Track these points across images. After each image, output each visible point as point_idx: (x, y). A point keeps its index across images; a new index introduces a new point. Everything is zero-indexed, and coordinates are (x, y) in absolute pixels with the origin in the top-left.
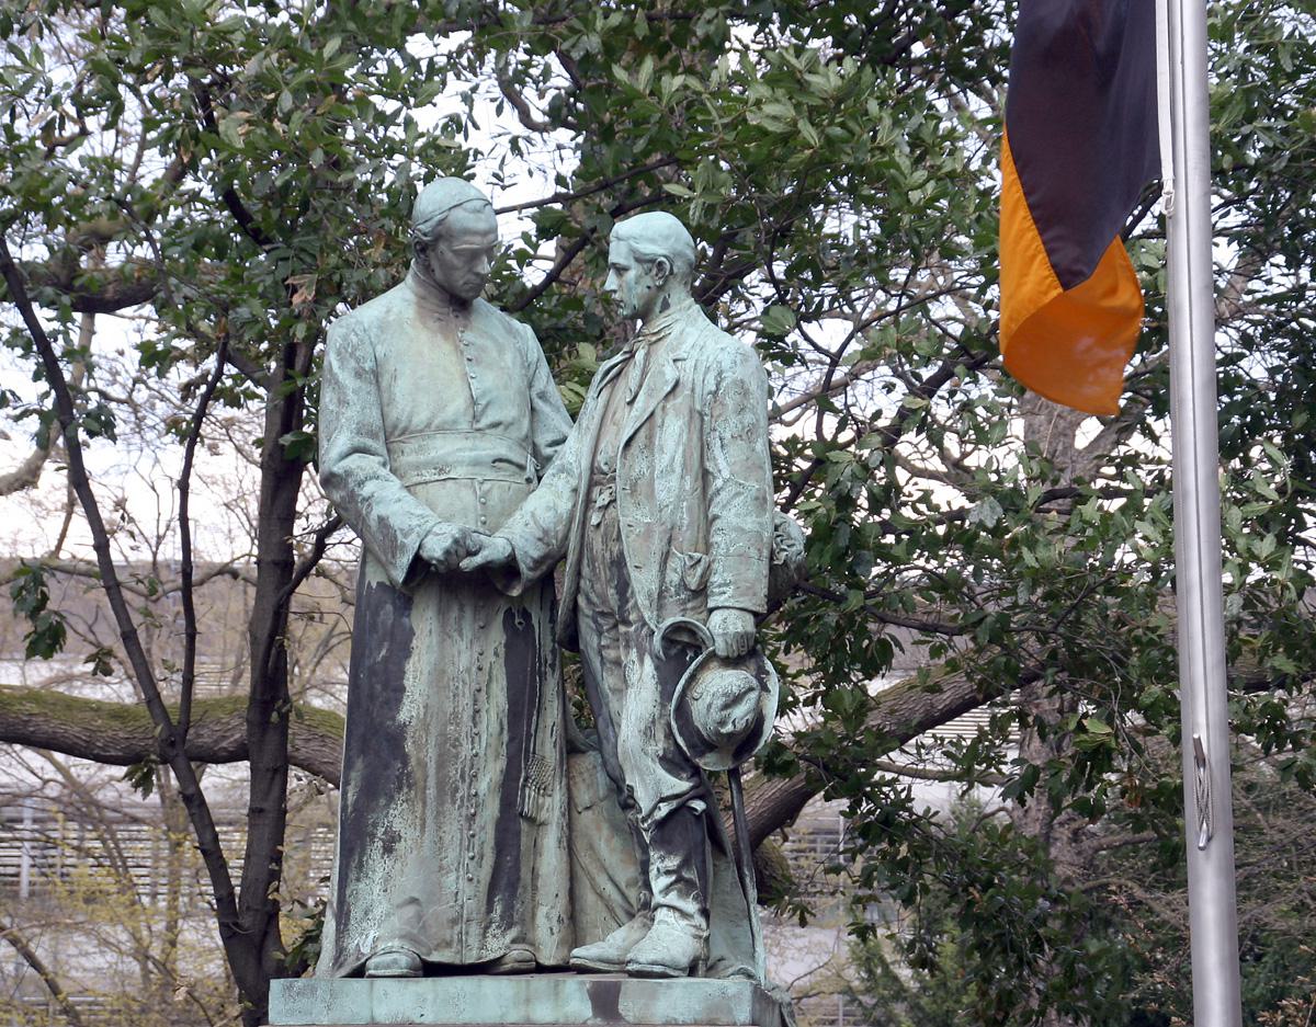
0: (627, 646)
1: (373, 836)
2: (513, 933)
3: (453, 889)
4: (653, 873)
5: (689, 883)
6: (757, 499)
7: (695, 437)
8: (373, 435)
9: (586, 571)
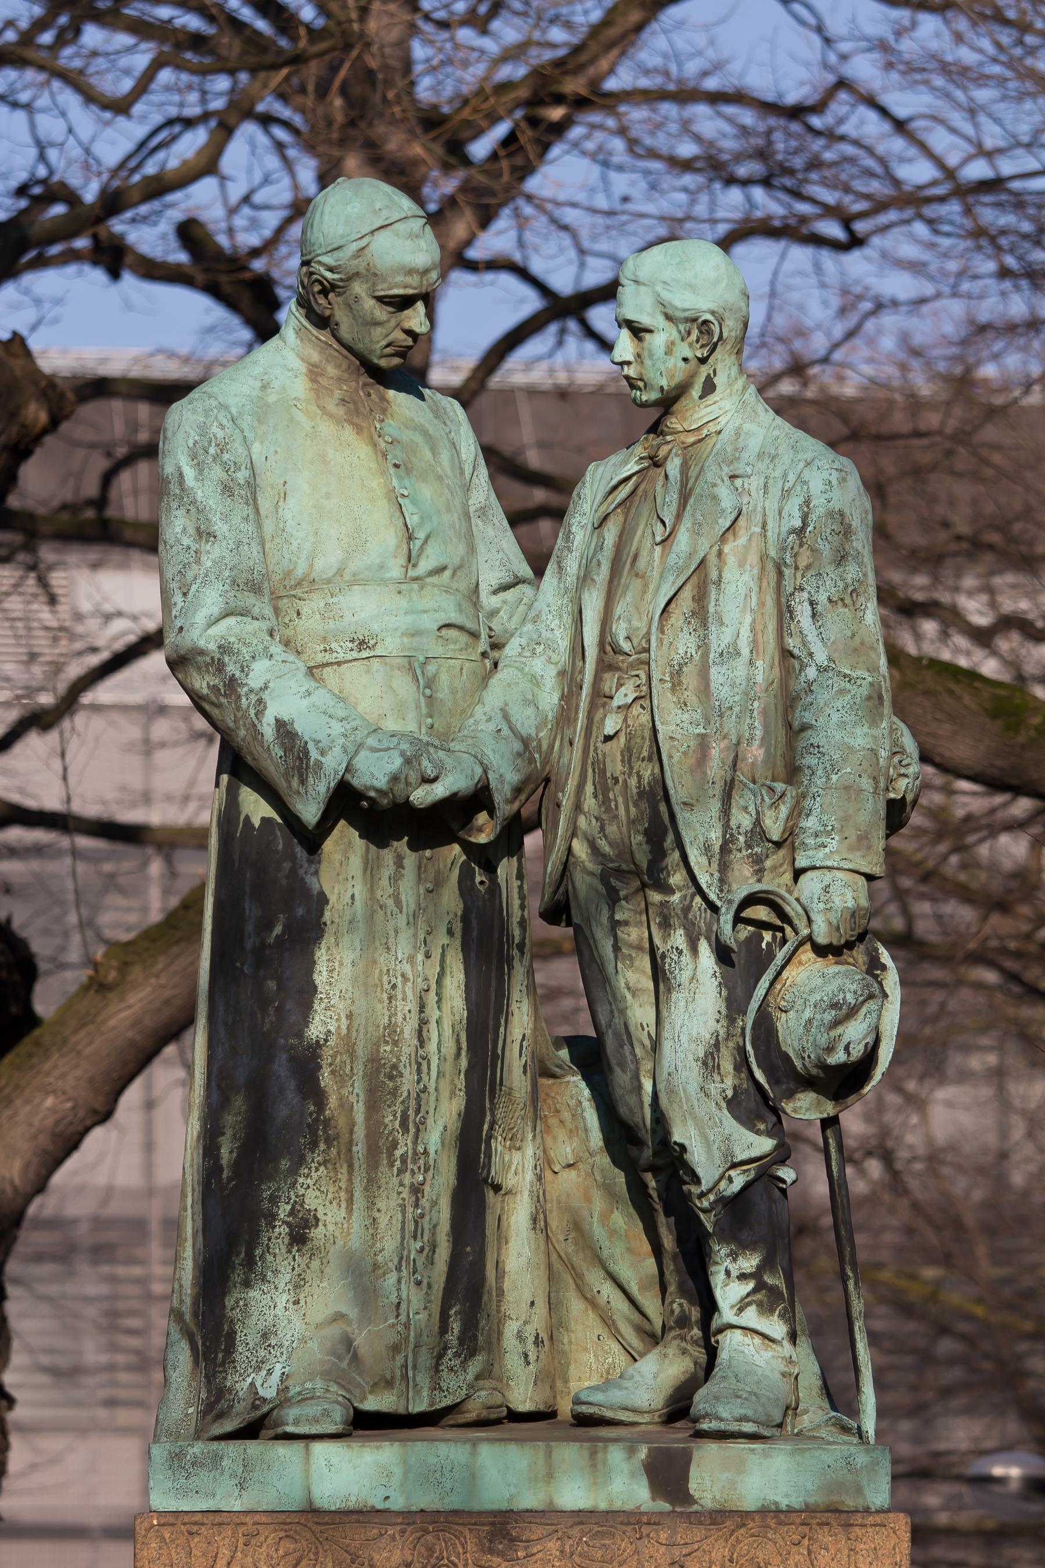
0: (666, 925)
1: (272, 1217)
3: (393, 1298)
4: (718, 1280)
5: (773, 1292)
6: (869, 698)
9: (590, 803)
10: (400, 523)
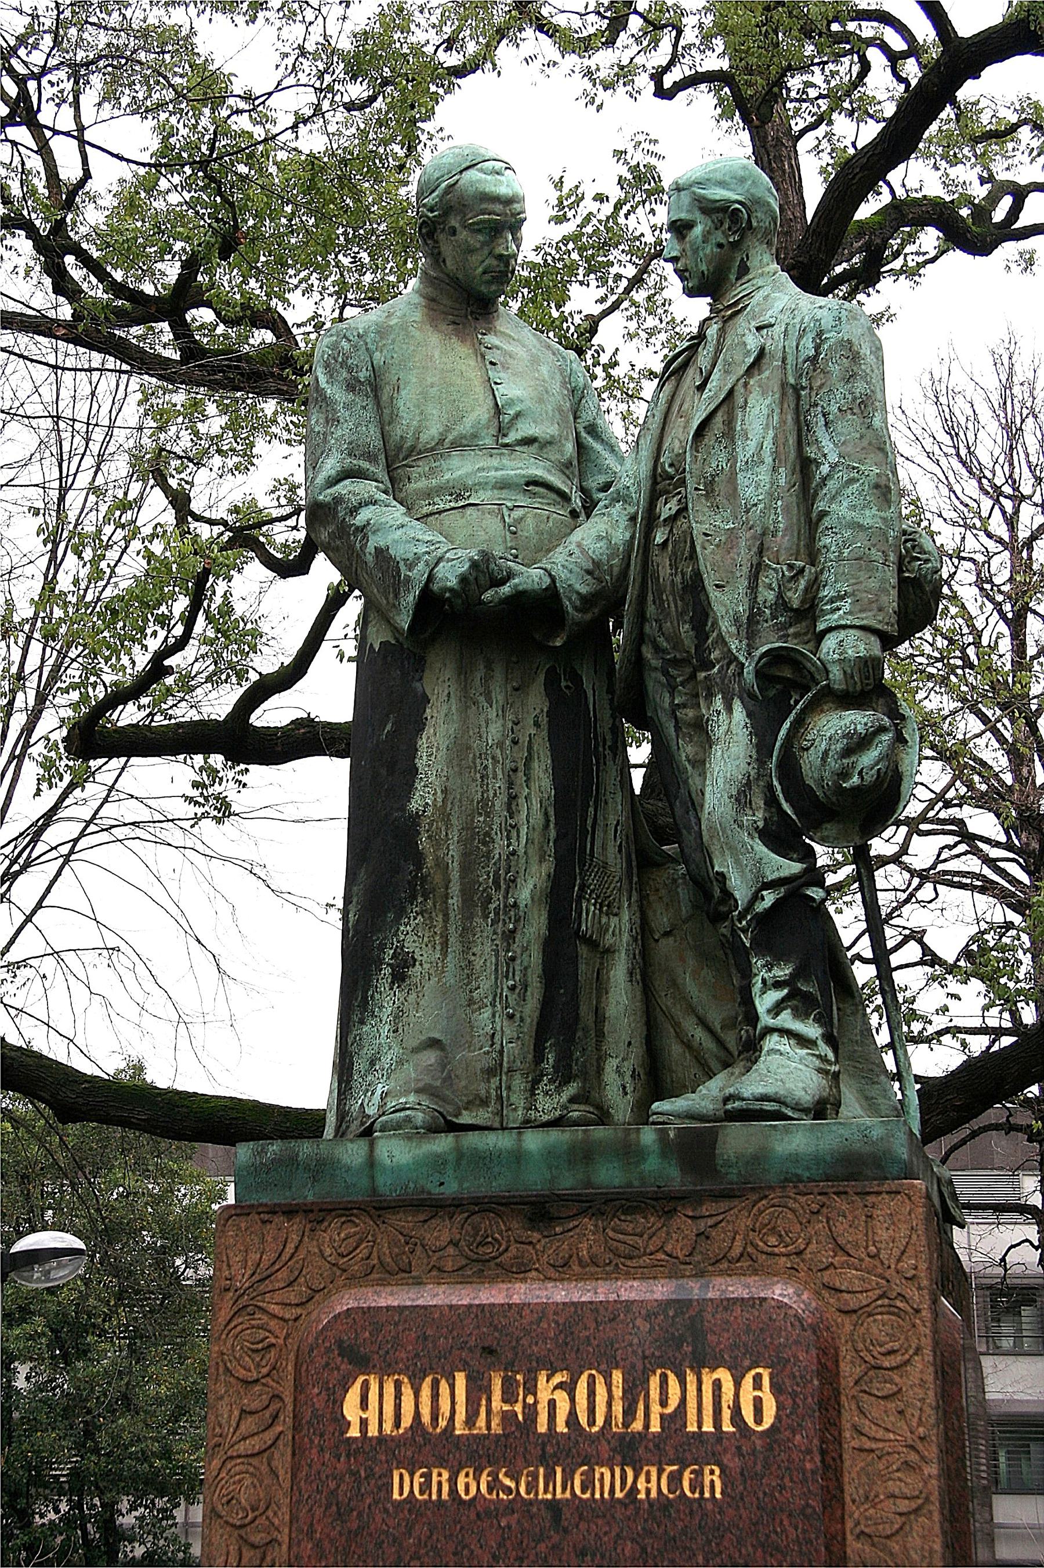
2: (571, 1089)
3: (488, 1029)
5: (807, 997)
6: (877, 486)
8: (371, 457)
9: (651, 610)
10: (491, 404)
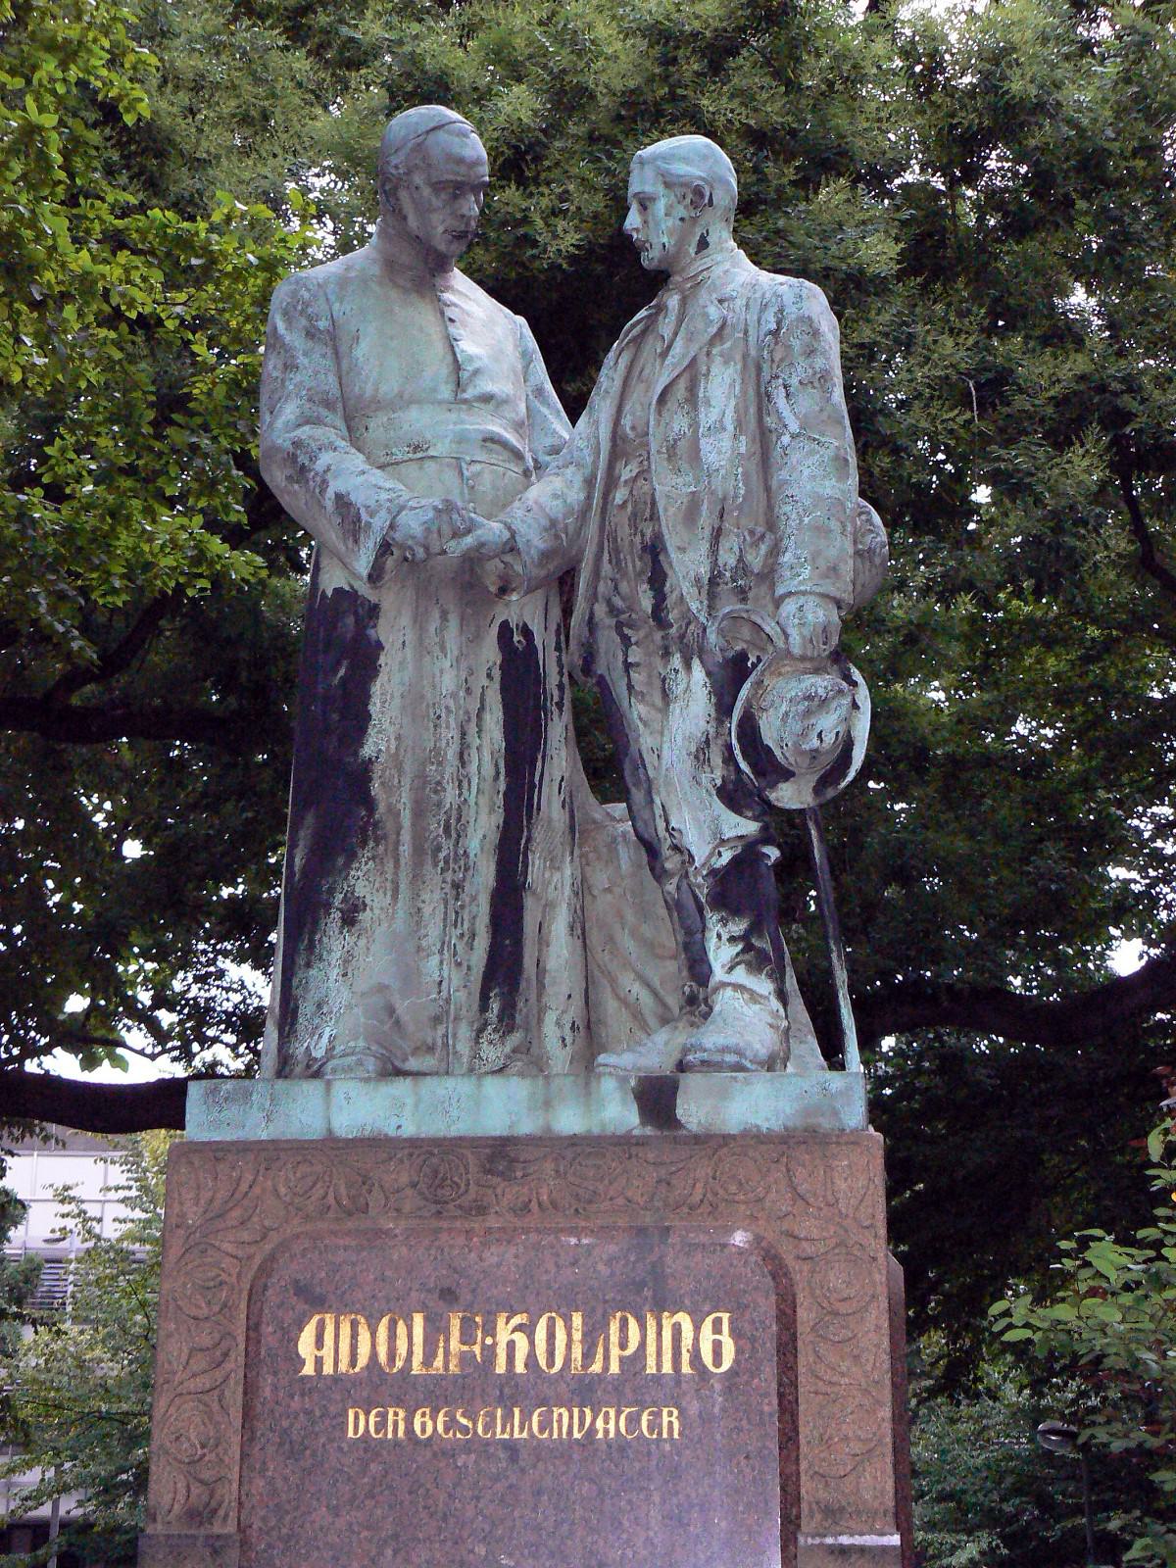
0: (666, 654)
1: (328, 906)
2: (516, 1038)
4: (712, 943)
7: (751, 392)
8: (328, 404)
9: (606, 568)
